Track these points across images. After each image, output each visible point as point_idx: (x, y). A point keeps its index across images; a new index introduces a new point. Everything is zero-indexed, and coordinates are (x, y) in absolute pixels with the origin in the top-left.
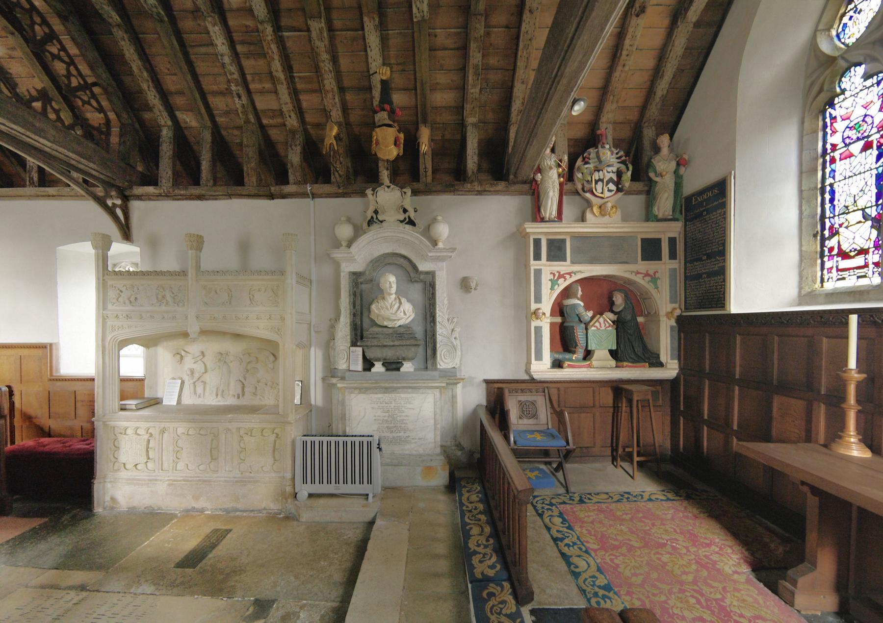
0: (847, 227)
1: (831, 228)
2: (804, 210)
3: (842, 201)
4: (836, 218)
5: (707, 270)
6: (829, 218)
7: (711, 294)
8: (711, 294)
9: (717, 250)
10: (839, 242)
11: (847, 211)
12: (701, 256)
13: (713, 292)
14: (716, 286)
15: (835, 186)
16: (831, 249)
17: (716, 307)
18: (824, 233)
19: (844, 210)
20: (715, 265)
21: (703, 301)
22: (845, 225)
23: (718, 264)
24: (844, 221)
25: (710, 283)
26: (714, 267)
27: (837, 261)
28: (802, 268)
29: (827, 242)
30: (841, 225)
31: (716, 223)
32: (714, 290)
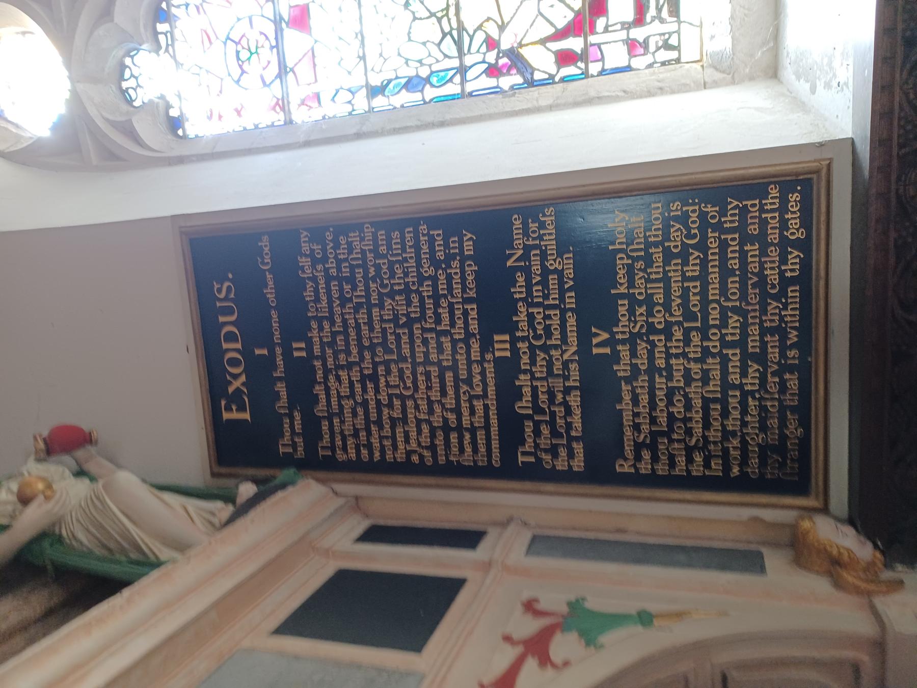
0: (502, 28)
1: (493, 71)
2: (419, 123)
3: (421, 53)
4: (468, 60)
5: (572, 321)
6: (463, 81)
7: (713, 291)
8: (713, 291)
9: (471, 268)
10: (543, 42)
11: (455, 33)
12: (490, 368)
13: (703, 278)
14: (668, 256)
15: (376, 81)
16: (565, 58)
17: (805, 246)
18: (506, 88)
19: (448, 43)
20: (545, 272)
21: (753, 345)
22: (494, 33)
23: (544, 256)
24: (480, 37)
25: (649, 302)
26: (560, 273)
27: (606, 30)
28: (622, 94)
29: (538, 76)
30: (491, 44)
31: (352, 280)
32: (693, 270)
